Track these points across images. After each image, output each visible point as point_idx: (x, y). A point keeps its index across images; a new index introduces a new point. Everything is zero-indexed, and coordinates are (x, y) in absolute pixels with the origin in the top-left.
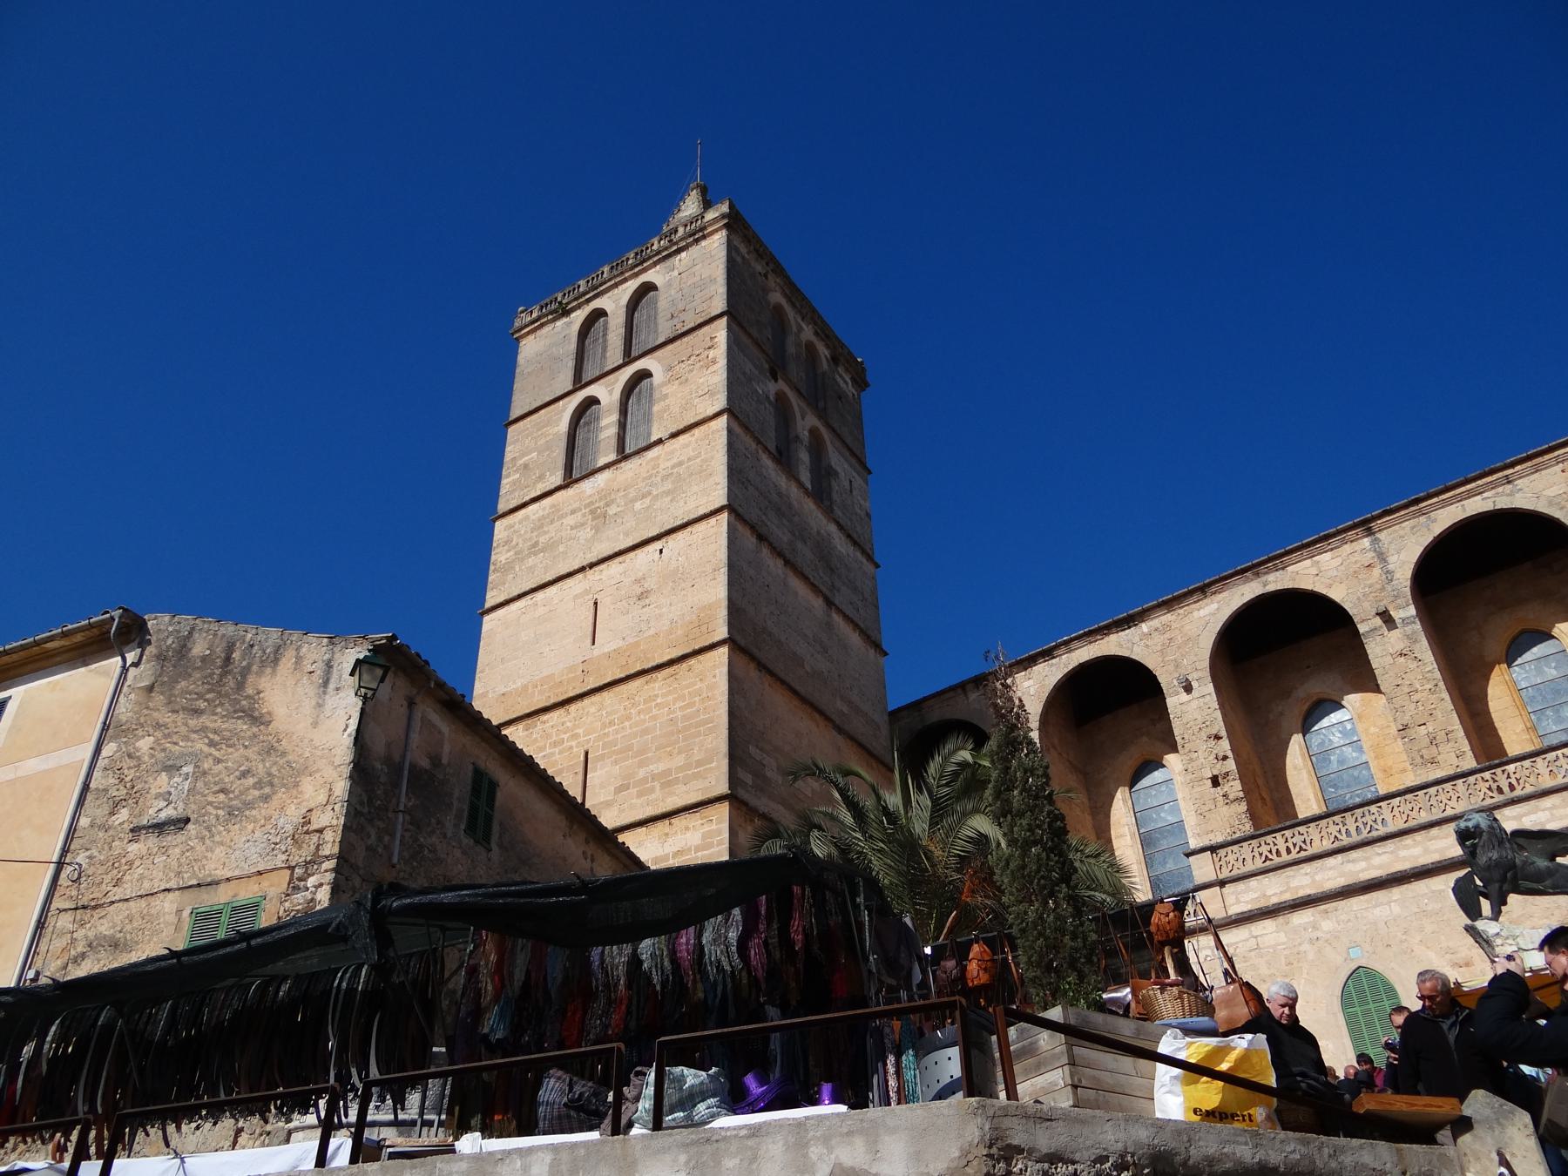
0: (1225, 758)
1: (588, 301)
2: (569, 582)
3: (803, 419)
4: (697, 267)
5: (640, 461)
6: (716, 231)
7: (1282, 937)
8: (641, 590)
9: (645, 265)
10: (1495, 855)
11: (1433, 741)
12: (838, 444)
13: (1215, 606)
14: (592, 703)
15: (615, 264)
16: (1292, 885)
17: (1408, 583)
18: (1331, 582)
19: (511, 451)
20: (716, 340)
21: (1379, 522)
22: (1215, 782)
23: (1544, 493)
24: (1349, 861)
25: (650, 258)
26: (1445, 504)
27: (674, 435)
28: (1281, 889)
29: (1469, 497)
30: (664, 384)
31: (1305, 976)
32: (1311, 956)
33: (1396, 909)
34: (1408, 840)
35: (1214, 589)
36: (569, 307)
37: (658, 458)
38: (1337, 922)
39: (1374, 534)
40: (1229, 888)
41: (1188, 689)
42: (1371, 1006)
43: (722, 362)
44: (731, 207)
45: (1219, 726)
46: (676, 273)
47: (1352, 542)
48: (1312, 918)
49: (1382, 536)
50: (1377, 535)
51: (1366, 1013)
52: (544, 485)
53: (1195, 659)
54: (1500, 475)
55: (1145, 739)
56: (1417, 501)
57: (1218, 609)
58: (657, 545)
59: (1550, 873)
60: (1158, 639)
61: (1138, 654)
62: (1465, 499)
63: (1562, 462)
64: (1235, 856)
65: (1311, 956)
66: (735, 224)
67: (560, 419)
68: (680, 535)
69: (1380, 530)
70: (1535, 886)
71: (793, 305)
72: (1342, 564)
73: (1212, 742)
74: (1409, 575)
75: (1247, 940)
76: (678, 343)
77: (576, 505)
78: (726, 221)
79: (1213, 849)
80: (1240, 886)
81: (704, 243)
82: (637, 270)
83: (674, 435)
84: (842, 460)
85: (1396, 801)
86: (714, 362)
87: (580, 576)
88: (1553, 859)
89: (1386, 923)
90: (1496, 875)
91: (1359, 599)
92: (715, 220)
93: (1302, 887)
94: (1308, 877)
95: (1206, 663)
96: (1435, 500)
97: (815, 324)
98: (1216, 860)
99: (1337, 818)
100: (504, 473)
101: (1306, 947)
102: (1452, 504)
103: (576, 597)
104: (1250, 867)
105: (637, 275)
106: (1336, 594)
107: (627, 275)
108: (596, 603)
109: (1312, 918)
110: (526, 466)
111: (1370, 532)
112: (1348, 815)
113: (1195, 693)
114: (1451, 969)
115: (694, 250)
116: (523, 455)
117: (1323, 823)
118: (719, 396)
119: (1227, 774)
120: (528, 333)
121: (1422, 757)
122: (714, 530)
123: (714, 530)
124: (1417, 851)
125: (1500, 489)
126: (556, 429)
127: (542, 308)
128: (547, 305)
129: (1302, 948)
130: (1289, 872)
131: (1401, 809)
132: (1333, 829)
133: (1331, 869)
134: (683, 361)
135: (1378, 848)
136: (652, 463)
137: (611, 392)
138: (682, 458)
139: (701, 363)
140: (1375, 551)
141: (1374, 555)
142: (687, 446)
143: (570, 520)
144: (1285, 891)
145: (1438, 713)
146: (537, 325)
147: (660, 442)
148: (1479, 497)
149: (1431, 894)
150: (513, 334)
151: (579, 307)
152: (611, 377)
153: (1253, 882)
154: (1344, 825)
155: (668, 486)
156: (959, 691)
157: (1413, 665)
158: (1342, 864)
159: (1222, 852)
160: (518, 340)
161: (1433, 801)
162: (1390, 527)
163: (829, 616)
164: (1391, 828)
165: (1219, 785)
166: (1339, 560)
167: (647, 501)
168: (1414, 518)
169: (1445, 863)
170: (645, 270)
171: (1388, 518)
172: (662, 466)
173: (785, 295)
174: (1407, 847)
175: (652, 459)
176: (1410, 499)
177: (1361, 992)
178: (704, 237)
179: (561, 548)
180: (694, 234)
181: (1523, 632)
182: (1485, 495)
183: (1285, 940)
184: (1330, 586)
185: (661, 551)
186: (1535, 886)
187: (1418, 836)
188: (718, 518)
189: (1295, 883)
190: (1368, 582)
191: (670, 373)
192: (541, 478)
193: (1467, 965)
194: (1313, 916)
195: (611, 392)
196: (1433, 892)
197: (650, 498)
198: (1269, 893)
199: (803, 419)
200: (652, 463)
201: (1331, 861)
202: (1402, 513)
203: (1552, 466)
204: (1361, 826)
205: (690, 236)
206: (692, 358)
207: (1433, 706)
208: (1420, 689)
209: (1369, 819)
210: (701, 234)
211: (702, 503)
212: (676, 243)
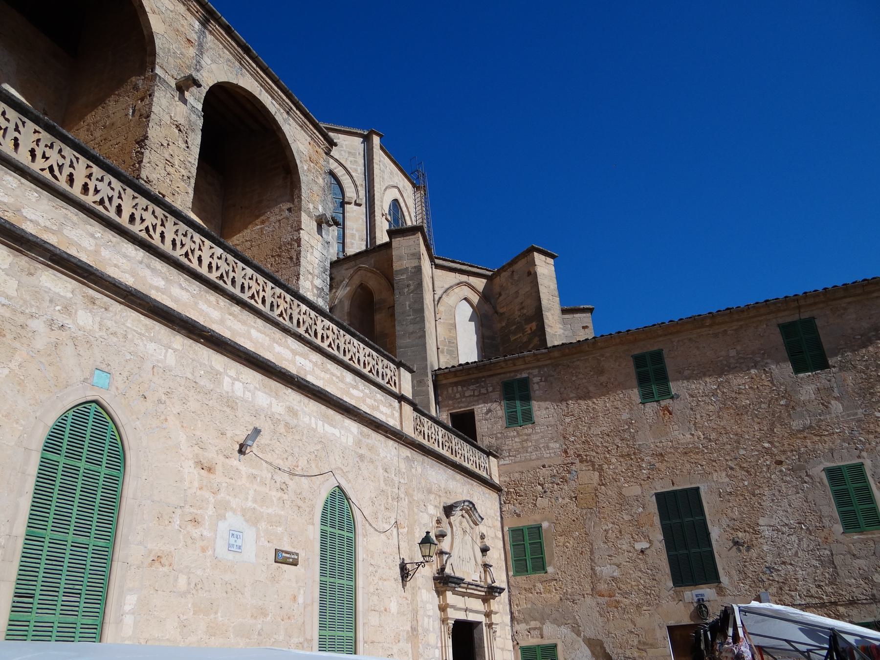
16: (65, 232)
18: (157, 12)
21: (217, 26)
24: (148, 266)
26: (255, 76)
28: (48, 224)
29: (267, 91)
31: (14, 365)
32: (40, 343)
38: (100, 325)
39: (205, 28)
42: (82, 465)
47: (188, 10)
48: (70, 295)
51: (71, 472)
54: (290, 104)
56: (247, 51)
62: (265, 89)
65: (40, 343)
69: (210, 32)
72: (171, 11)
74: (211, 85)
89: (153, 367)
93: (79, 247)
94: (92, 241)
96: (254, 66)
102: (257, 81)
109: (70, 295)
111: (204, 23)
114: (193, 466)
125: (282, 111)
129: (34, 324)
140: (199, 38)
141: (197, 39)
144: (54, 232)
149: (209, 370)
158: (141, 262)
162: (217, 39)
166: (171, 7)
168: (234, 56)
169: (241, 349)
171: (223, 33)
176: (247, 44)
177: (77, 437)
183: (15, 294)
184: (154, 12)
190: (183, 50)
193: (210, 470)
194: (72, 292)
196: (212, 367)
198: (26, 212)
202: (233, 44)
203: (308, 134)
207: (177, 189)
208: (177, 167)
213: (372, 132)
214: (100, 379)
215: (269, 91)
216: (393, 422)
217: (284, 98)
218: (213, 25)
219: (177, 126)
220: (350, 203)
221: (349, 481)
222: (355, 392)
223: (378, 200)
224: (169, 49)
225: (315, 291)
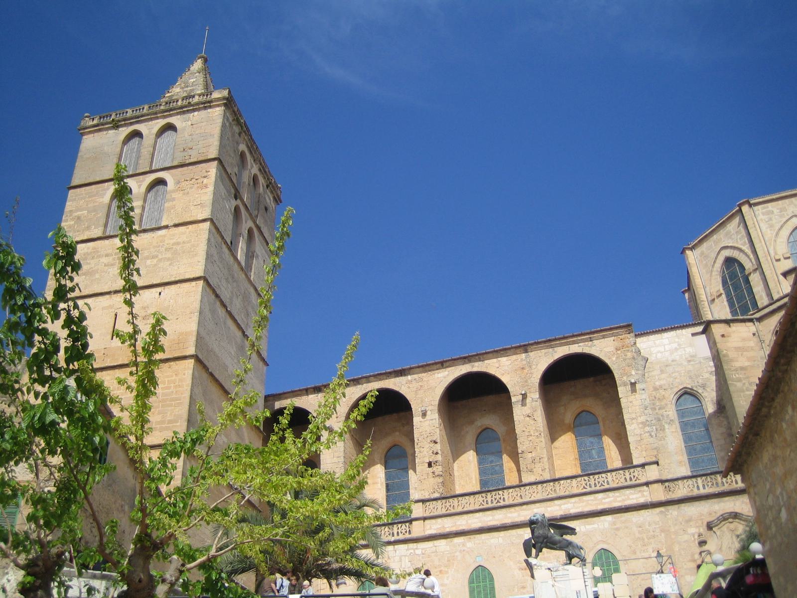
0: (437, 453)
1: (131, 124)
2: (100, 298)
3: (246, 222)
4: (204, 124)
5: (153, 235)
6: (218, 106)
7: (448, 548)
8: (145, 314)
9: (171, 112)
10: (541, 532)
11: (533, 461)
12: (261, 238)
13: (446, 373)
14: (108, 375)
15: (152, 105)
17: (538, 381)
19: (69, 205)
20: (209, 173)
22: (430, 465)
23: (605, 349)
25: (175, 109)
27: (176, 226)
30: (174, 191)
33: (501, 540)
34: (512, 509)
35: (448, 364)
36: (120, 123)
37: (165, 236)
40: (427, 522)
41: (424, 414)
42: (481, 584)
43: (211, 188)
44: (230, 92)
45: (437, 437)
46: (190, 123)
49: (531, 354)
50: (529, 353)
52: (90, 233)
53: (432, 399)
54: (588, 336)
55: (397, 433)
56: (550, 341)
57: (448, 375)
58: (159, 289)
59: (560, 542)
60: (415, 385)
61: (404, 391)
63: (615, 336)
64: (433, 506)
66: (229, 103)
67: (105, 194)
68: (173, 287)
70: (551, 546)
71: (251, 153)
73: (432, 445)
75: (431, 547)
76: (185, 168)
77: (110, 251)
78: (225, 102)
79: (423, 501)
80: (433, 521)
81: (209, 110)
82: (165, 114)
83: (176, 226)
84: (262, 247)
85: (511, 490)
86: (206, 186)
87: (108, 296)
88: (562, 536)
90: (541, 540)
91: (515, 384)
92: (218, 99)
95: (437, 403)
97: (261, 164)
98: (424, 507)
99: (484, 495)
100: (64, 218)
101: (458, 554)
103: (103, 308)
104: (439, 512)
105: (165, 117)
106: (505, 379)
107: (159, 115)
108: (116, 315)
110: (79, 218)
112: (489, 494)
113: (428, 417)
115: (203, 113)
116: (77, 210)
117: (477, 496)
118: (206, 209)
119: (436, 462)
120: (90, 132)
121: (527, 468)
122: (194, 289)
123: (194, 289)
124: (515, 515)
125: (587, 343)
126: (101, 200)
127: (100, 118)
128: (104, 117)
130: (457, 517)
131: (512, 494)
132: (481, 499)
133: (476, 518)
134: (187, 180)
135: (498, 512)
136: (161, 238)
137: (140, 186)
138: (179, 240)
139: (198, 185)
142: (183, 233)
143: (105, 260)
145: (538, 448)
146: (98, 128)
147: (166, 227)
148: (577, 345)
150: (79, 130)
151: (125, 125)
152: (141, 177)
153: (439, 520)
154: (486, 498)
155: (169, 255)
156: (304, 392)
157: (532, 422)
159: (428, 504)
160: (83, 134)
161: (527, 493)
163: (243, 342)
164: (507, 503)
165: (431, 467)
167: (155, 261)
170: (171, 116)
172: (166, 242)
173: (248, 147)
174: (511, 512)
175: (161, 236)
178: (210, 107)
179: (97, 276)
180: (204, 103)
181: (583, 411)
182: (580, 344)
184: (503, 374)
185: (160, 294)
186: (551, 546)
187: (517, 508)
188: (197, 282)
189: (459, 523)
191: (178, 186)
192: (88, 228)
195: (140, 186)
197: (157, 259)
199: (246, 222)
200: (161, 238)
201: (477, 515)
204: (494, 500)
205: (202, 104)
206: (194, 180)
209: (498, 497)
210: (209, 104)
211: (188, 271)
212: (193, 105)
213: (740, 206)
214: (478, 559)
215: (574, 343)
216: (642, 500)
217: (583, 337)
218: (529, 349)
219: (528, 416)
220: (750, 274)
221: (608, 544)
222: (607, 500)
223: (763, 257)
224: (515, 384)
225: (640, 426)
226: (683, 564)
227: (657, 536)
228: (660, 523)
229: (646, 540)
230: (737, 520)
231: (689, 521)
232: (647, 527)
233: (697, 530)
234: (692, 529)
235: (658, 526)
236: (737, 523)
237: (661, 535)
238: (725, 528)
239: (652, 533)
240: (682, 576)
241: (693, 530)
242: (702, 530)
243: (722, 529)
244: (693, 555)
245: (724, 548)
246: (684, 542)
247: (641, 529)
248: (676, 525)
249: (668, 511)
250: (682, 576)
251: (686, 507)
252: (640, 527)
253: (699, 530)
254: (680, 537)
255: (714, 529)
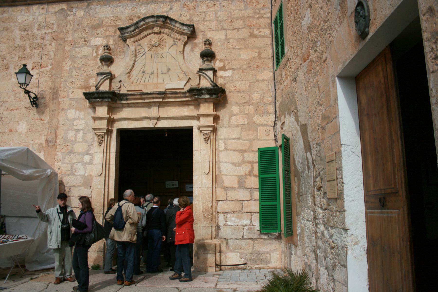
226: (71, 90)
227: (46, 46)
228: (55, 27)
229: (28, 50)
230: (166, 31)
231: (95, 27)
232: (35, 31)
233: (105, 43)
234: (98, 39)
235: (50, 31)
236: (165, 36)
237: (50, 45)
238: (144, 43)
239: (39, 41)
240: (63, 109)
241: (99, 41)
242: (111, 42)
243: (140, 42)
244: (88, 78)
245: (134, 73)
246: (81, 58)
247: (24, 33)
248: (75, 31)
249: (71, 9)
250: (63, 109)
251: (99, 7)
252: (25, 30)
253: (108, 41)
254: (77, 49)
255: (128, 41)
